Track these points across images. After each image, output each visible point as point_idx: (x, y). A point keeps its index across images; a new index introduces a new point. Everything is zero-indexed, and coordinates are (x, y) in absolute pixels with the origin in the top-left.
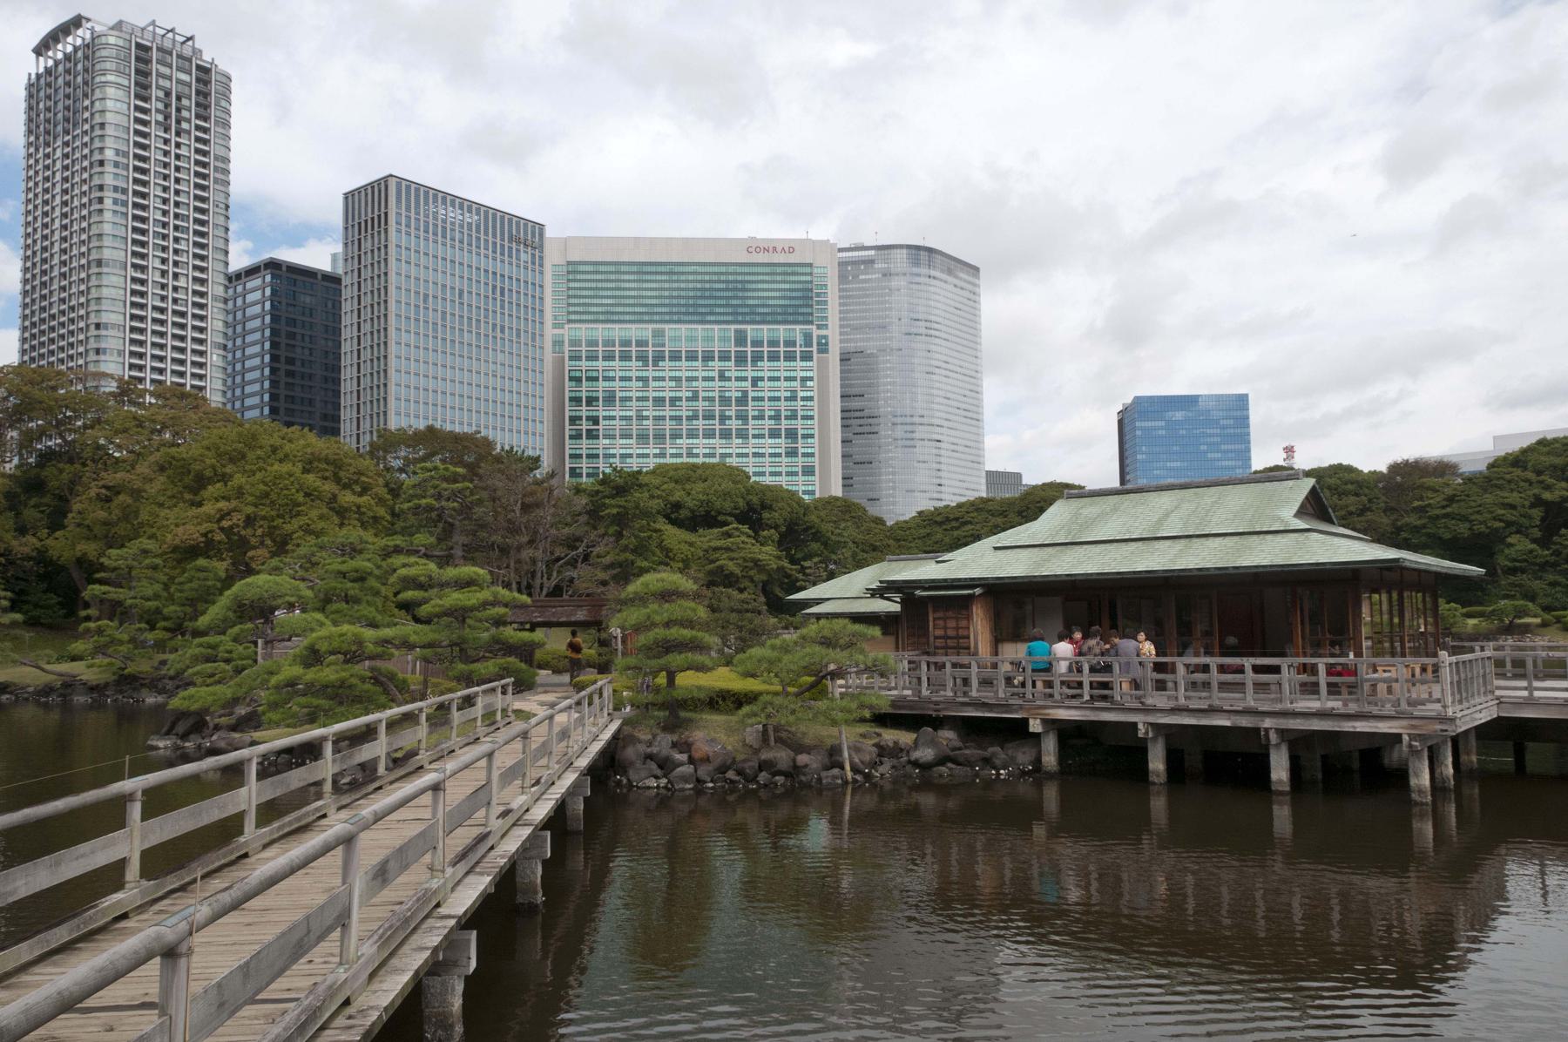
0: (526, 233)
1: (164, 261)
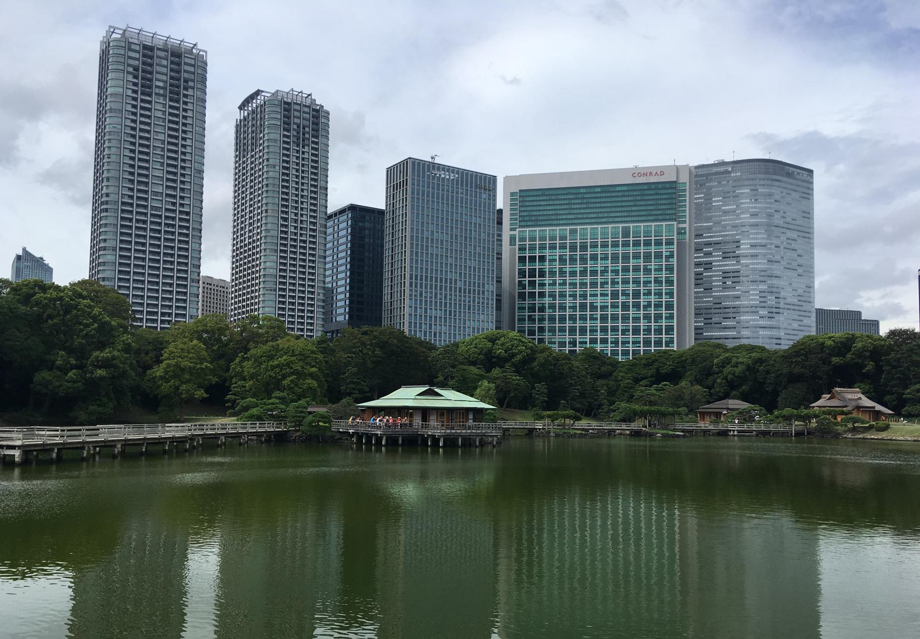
0: (485, 183)
1: (296, 214)
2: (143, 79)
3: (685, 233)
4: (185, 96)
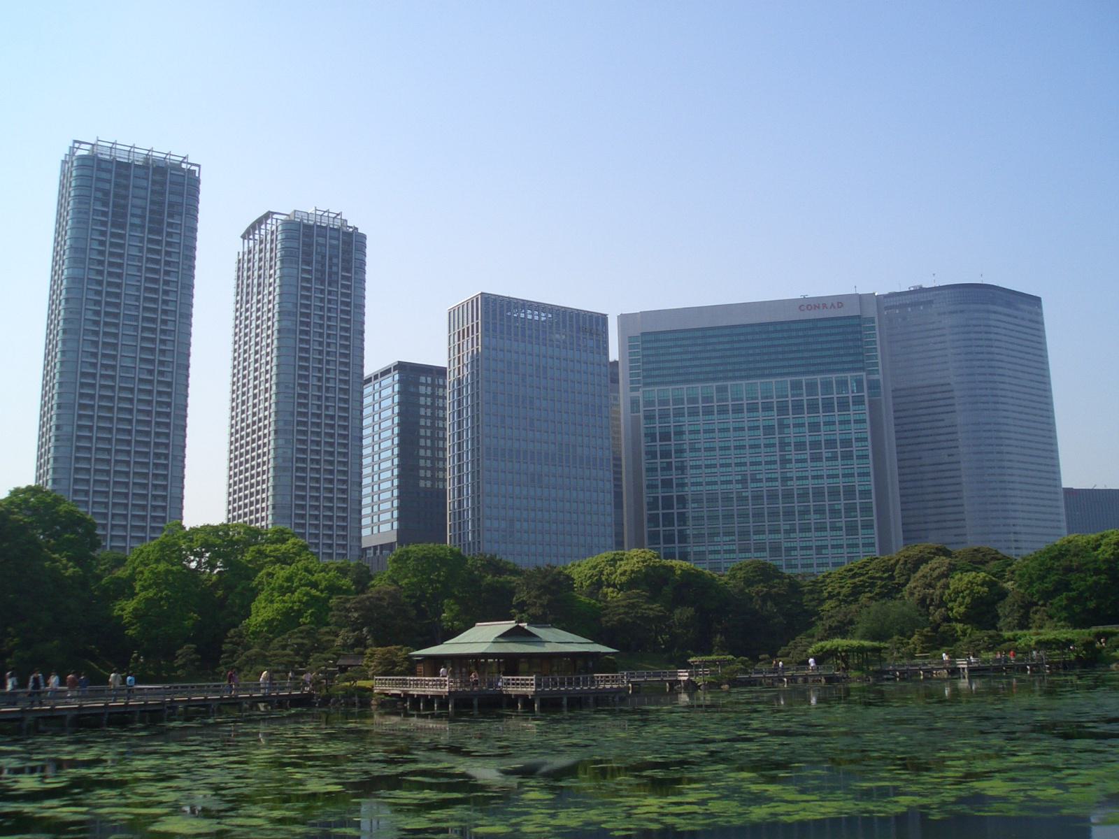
1: (320, 379)
2: (115, 205)
3: (878, 387)
4: (170, 225)
